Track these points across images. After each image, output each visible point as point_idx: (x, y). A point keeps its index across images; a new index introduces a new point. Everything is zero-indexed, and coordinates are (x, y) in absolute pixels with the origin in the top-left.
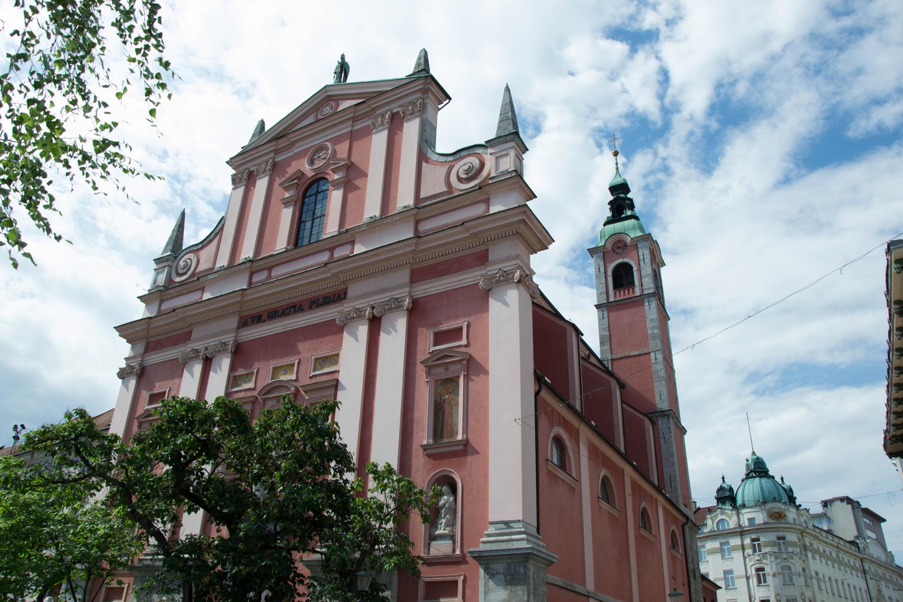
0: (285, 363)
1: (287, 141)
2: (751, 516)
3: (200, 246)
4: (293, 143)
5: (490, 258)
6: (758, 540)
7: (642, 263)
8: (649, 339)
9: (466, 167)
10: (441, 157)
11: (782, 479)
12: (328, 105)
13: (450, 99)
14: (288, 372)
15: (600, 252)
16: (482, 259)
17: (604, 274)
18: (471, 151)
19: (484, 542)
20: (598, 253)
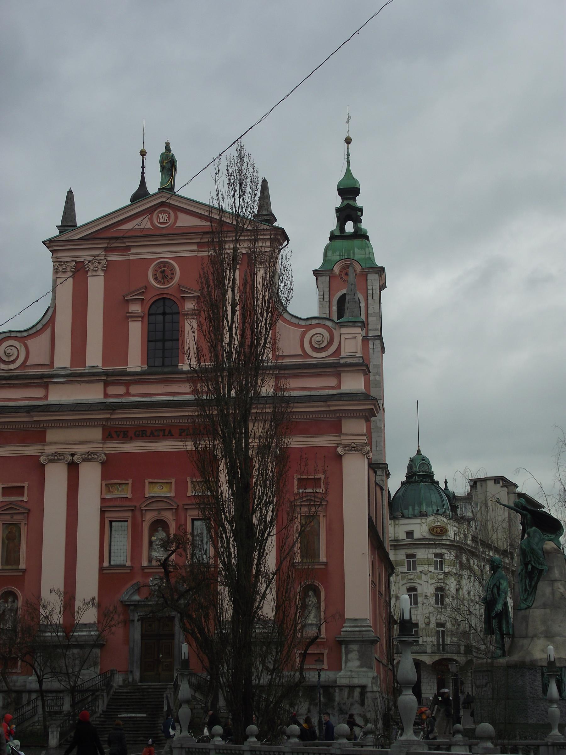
0: (161, 480)
1: (121, 243)
2: (409, 528)
3: (25, 334)
4: (128, 248)
5: (344, 430)
6: (414, 556)
7: (370, 298)
8: (371, 385)
9: (319, 338)
10: (293, 318)
11: (446, 483)
12: (164, 212)
13: (288, 240)
14: (164, 488)
15: (326, 276)
16: (336, 429)
17: (328, 303)
18: (321, 322)
19: (343, 631)
20: (323, 276)
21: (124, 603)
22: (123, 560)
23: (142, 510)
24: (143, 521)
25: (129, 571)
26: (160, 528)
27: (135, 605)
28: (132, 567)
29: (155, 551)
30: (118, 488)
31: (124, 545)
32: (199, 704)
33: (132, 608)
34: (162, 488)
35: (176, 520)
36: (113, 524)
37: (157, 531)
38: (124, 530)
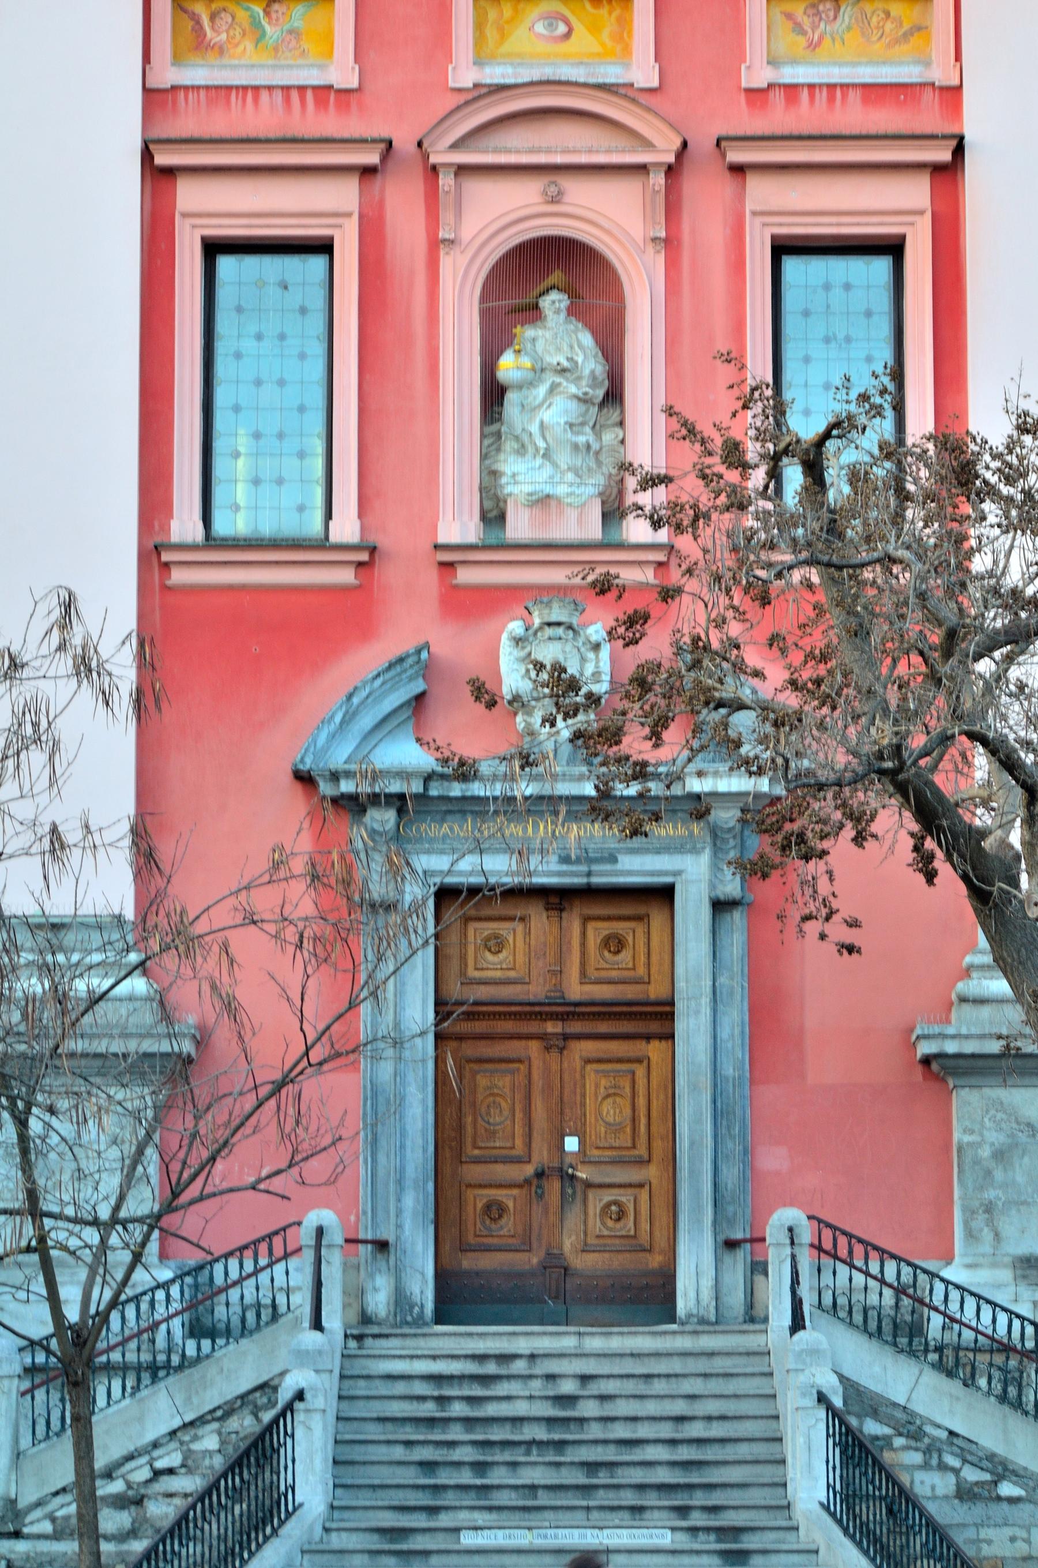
21: (326, 788)
22: (301, 509)
23: (434, 168)
24: (435, 245)
25: (346, 576)
26: (554, 295)
27: (399, 802)
28: (373, 550)
29: (521, 451)
30: (256, 25)
31: (302, 409)
32: (943, 1467)
33: (384, 818)
34: (562, 28)
35: (670, 244)
36: (225, 264)
37: (532, 313)
38: (303, 311)
